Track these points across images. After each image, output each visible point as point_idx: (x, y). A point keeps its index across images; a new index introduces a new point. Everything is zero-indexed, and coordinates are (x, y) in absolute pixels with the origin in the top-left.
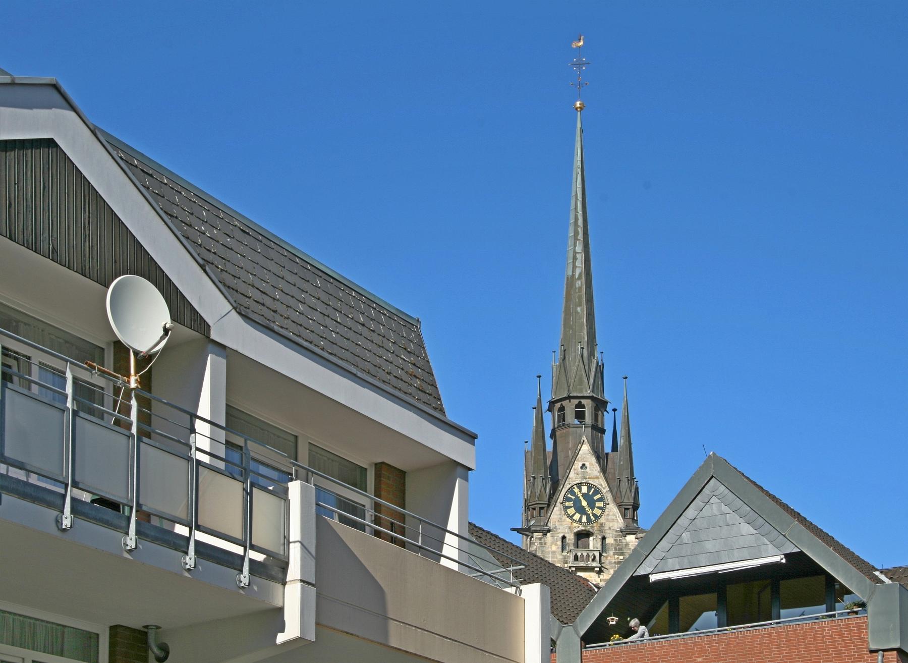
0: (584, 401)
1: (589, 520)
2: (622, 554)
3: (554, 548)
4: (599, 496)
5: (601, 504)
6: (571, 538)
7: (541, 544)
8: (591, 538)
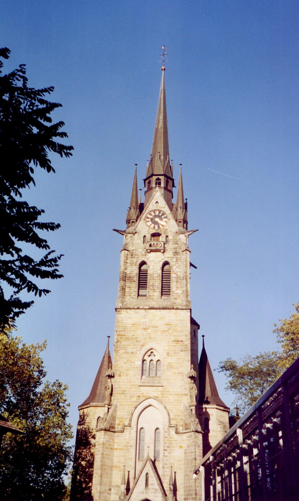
0: (160, 177)
1: (159, 227)
2: (177, 244)
3: (139, 241)
5: (165, 220)
6: (148, 237)
7: (132, 239)
8: (160, 237)
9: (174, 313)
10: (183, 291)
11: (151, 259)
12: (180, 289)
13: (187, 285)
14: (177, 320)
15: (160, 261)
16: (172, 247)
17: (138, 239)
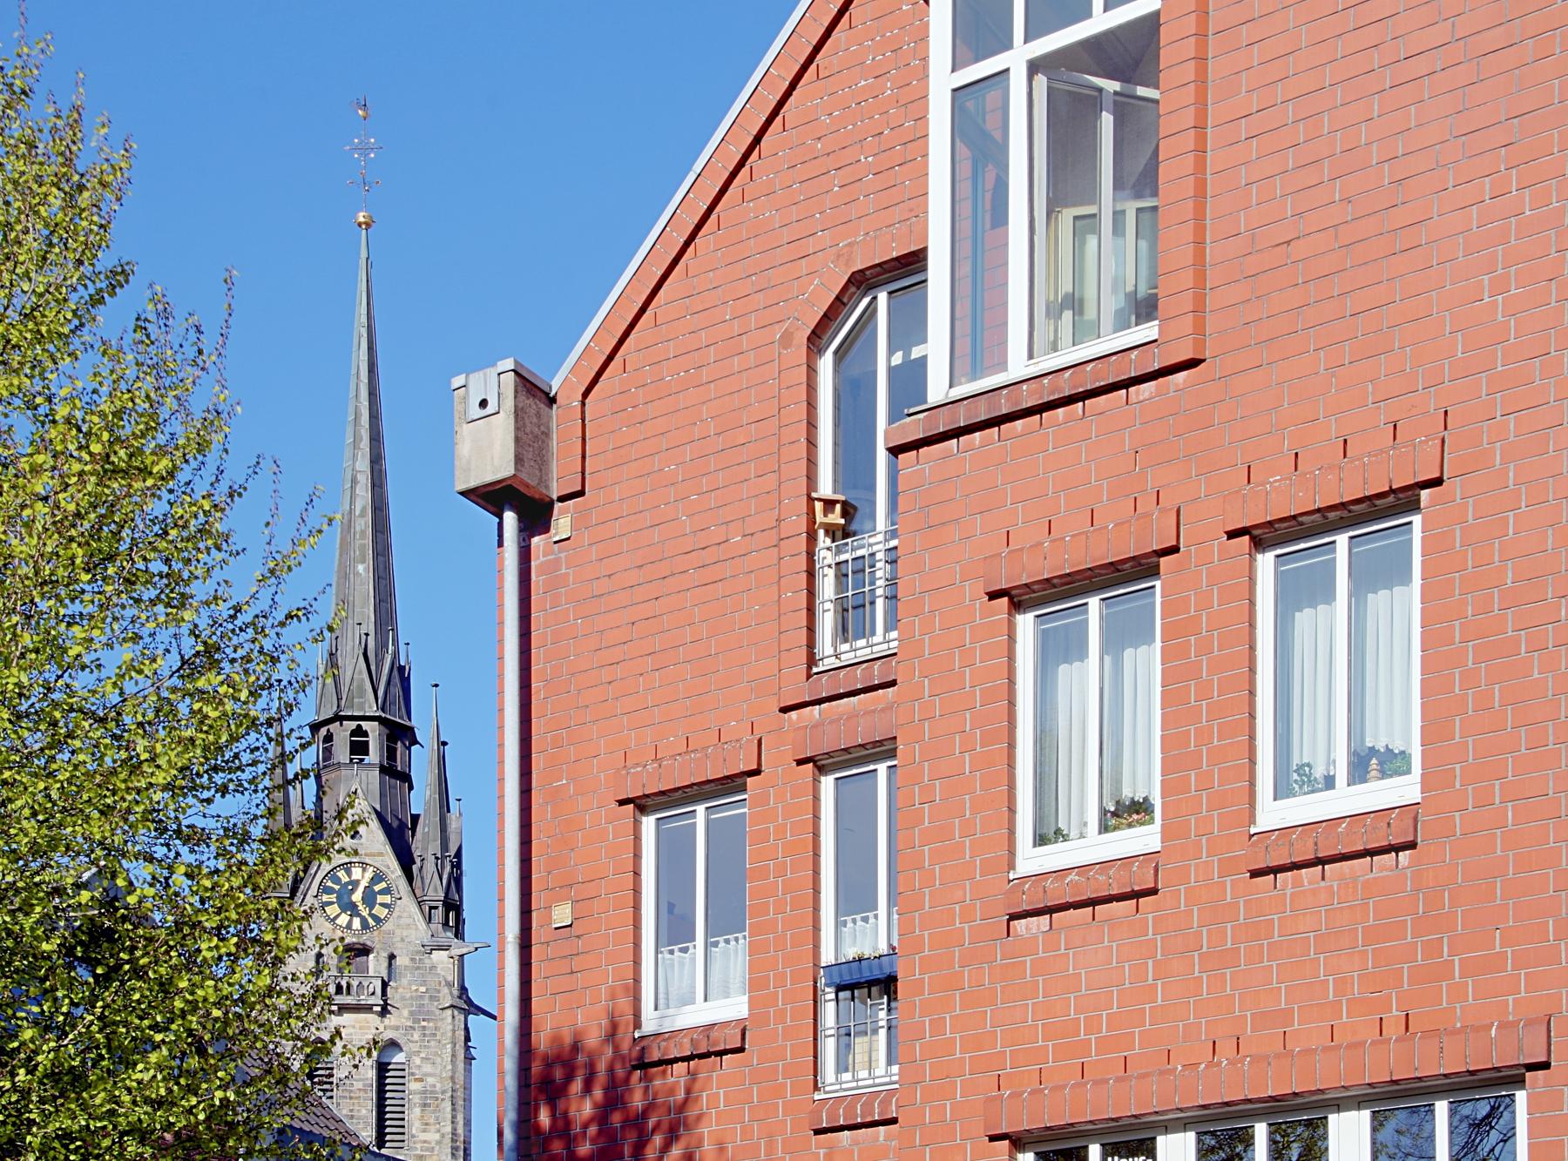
0: (365, 725)
1: (365, 925)
4: (383, 885)
5: (387, 899)
8: (371, 956)
10: (443, 1136)
12: (433, 1128)
13: (454, 1117)
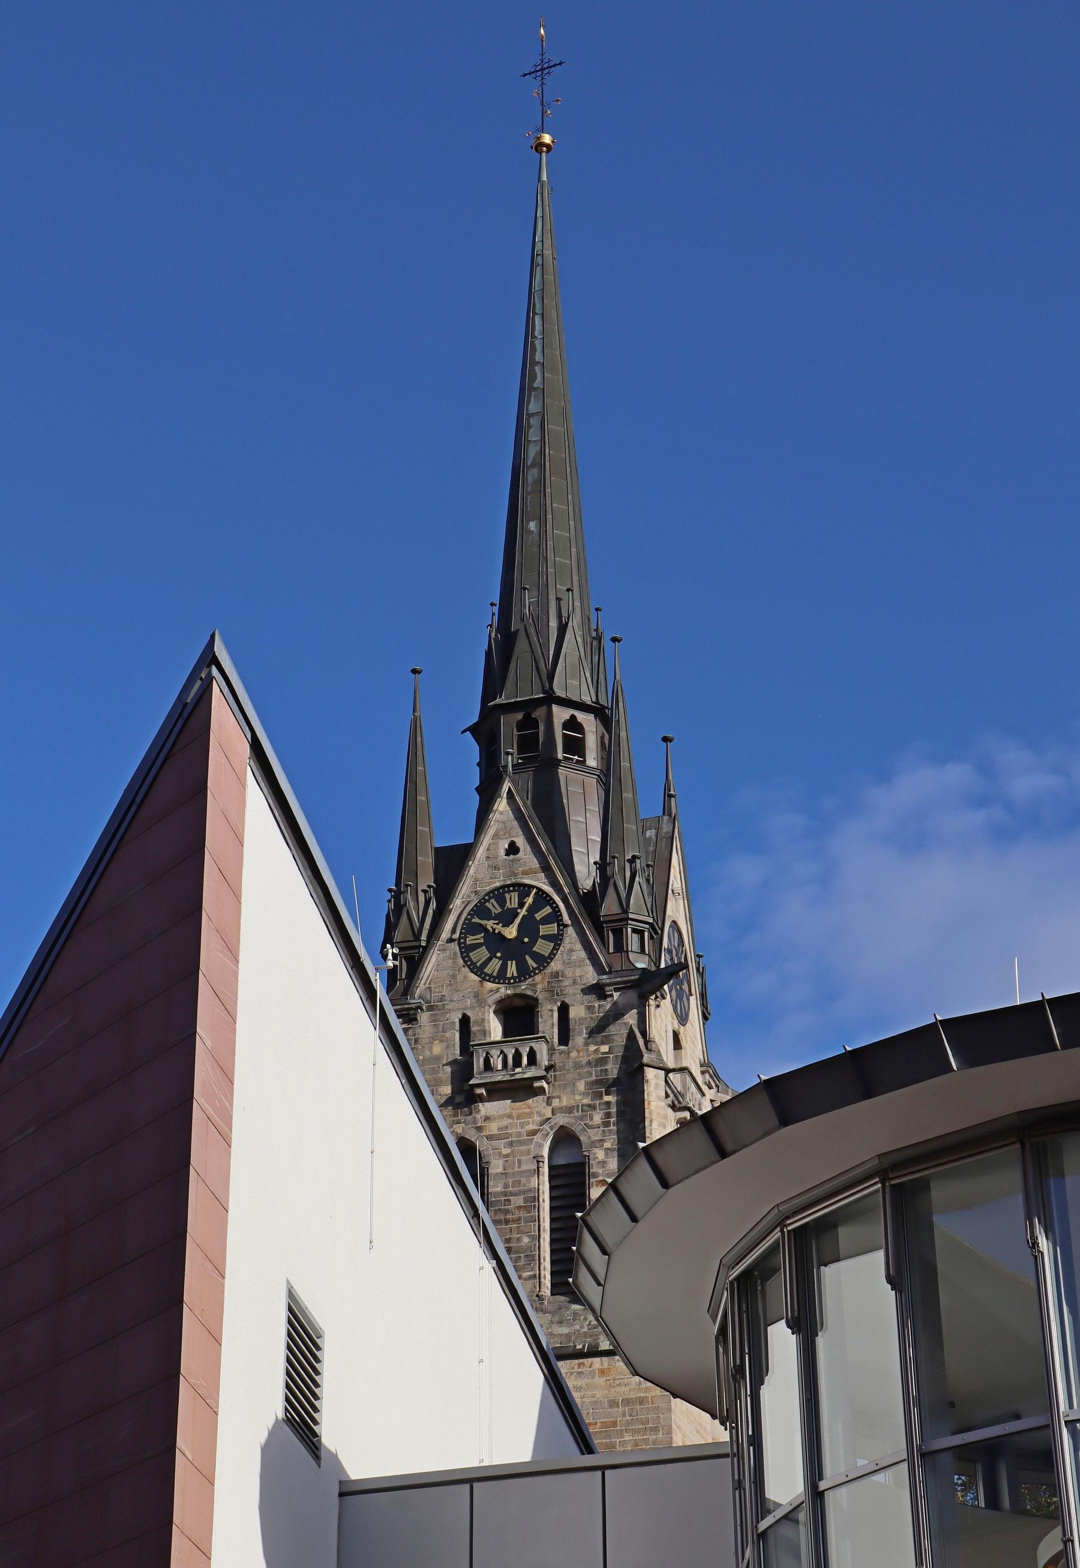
5: (553, 929)
9: (602, 1372)
11: (493, 1128)
14: (613, 1404)
15: (534, 1133)
16: (584, 1060)
17: (432, 1039)
